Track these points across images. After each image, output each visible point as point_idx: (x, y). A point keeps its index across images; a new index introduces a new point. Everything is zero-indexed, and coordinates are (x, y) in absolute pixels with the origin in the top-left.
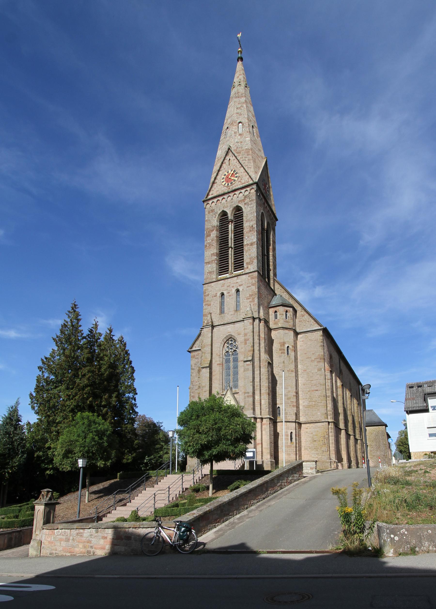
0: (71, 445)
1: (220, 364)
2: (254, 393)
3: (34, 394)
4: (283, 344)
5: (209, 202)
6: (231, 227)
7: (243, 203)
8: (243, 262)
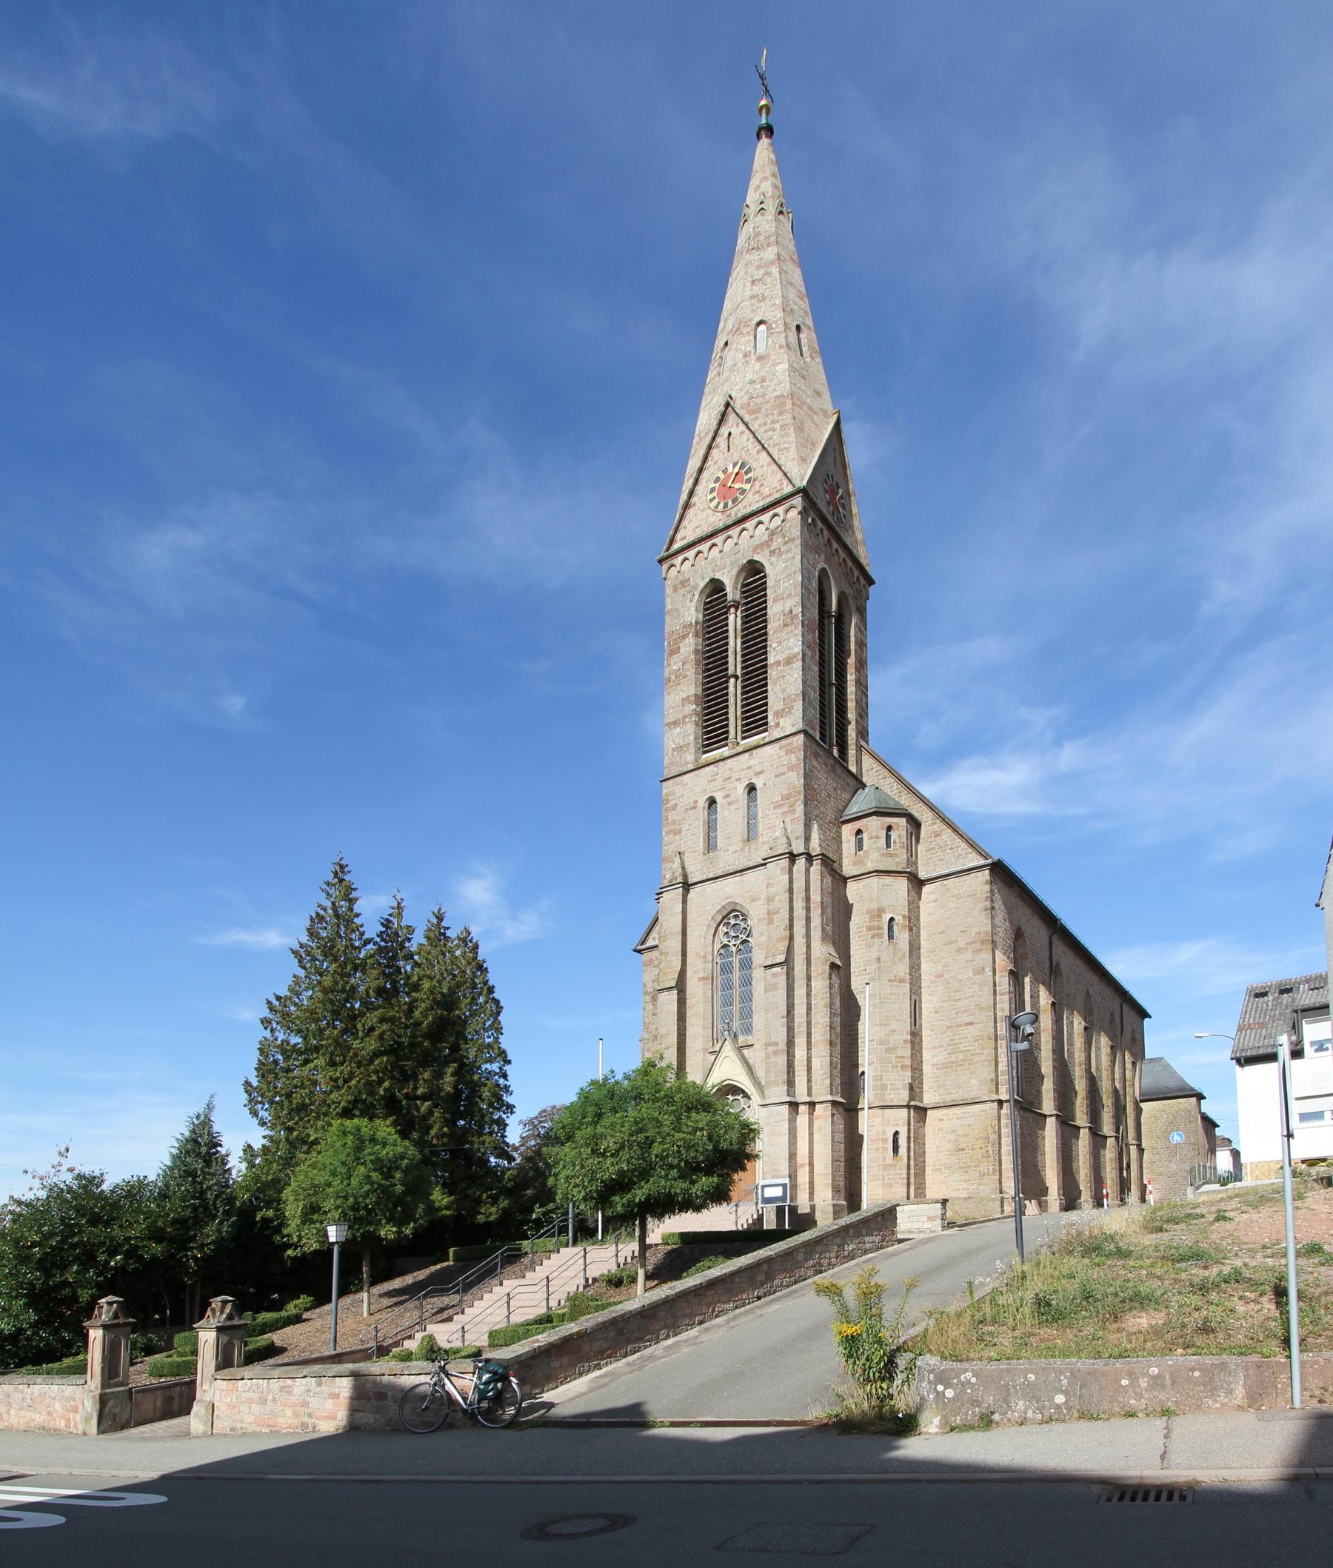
0: (316, 1193)
1: (704, 978)
2: (791, 1043)
3: (255, 1084)
4: (880, 912)
6: (734, 620)
7: (767, 552)
8: (766, 711)
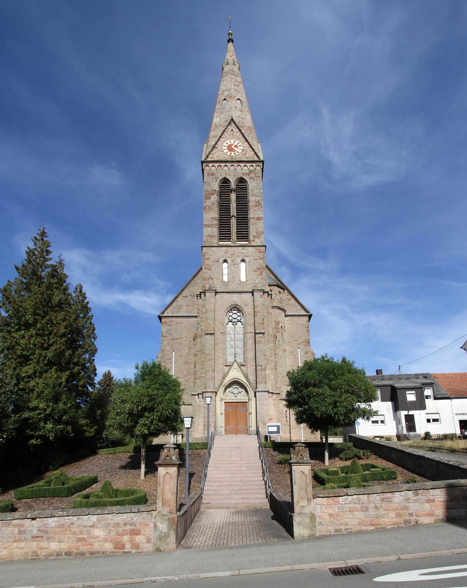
5: (209, 165)
6: (233, 196)
7: (248, 177)
